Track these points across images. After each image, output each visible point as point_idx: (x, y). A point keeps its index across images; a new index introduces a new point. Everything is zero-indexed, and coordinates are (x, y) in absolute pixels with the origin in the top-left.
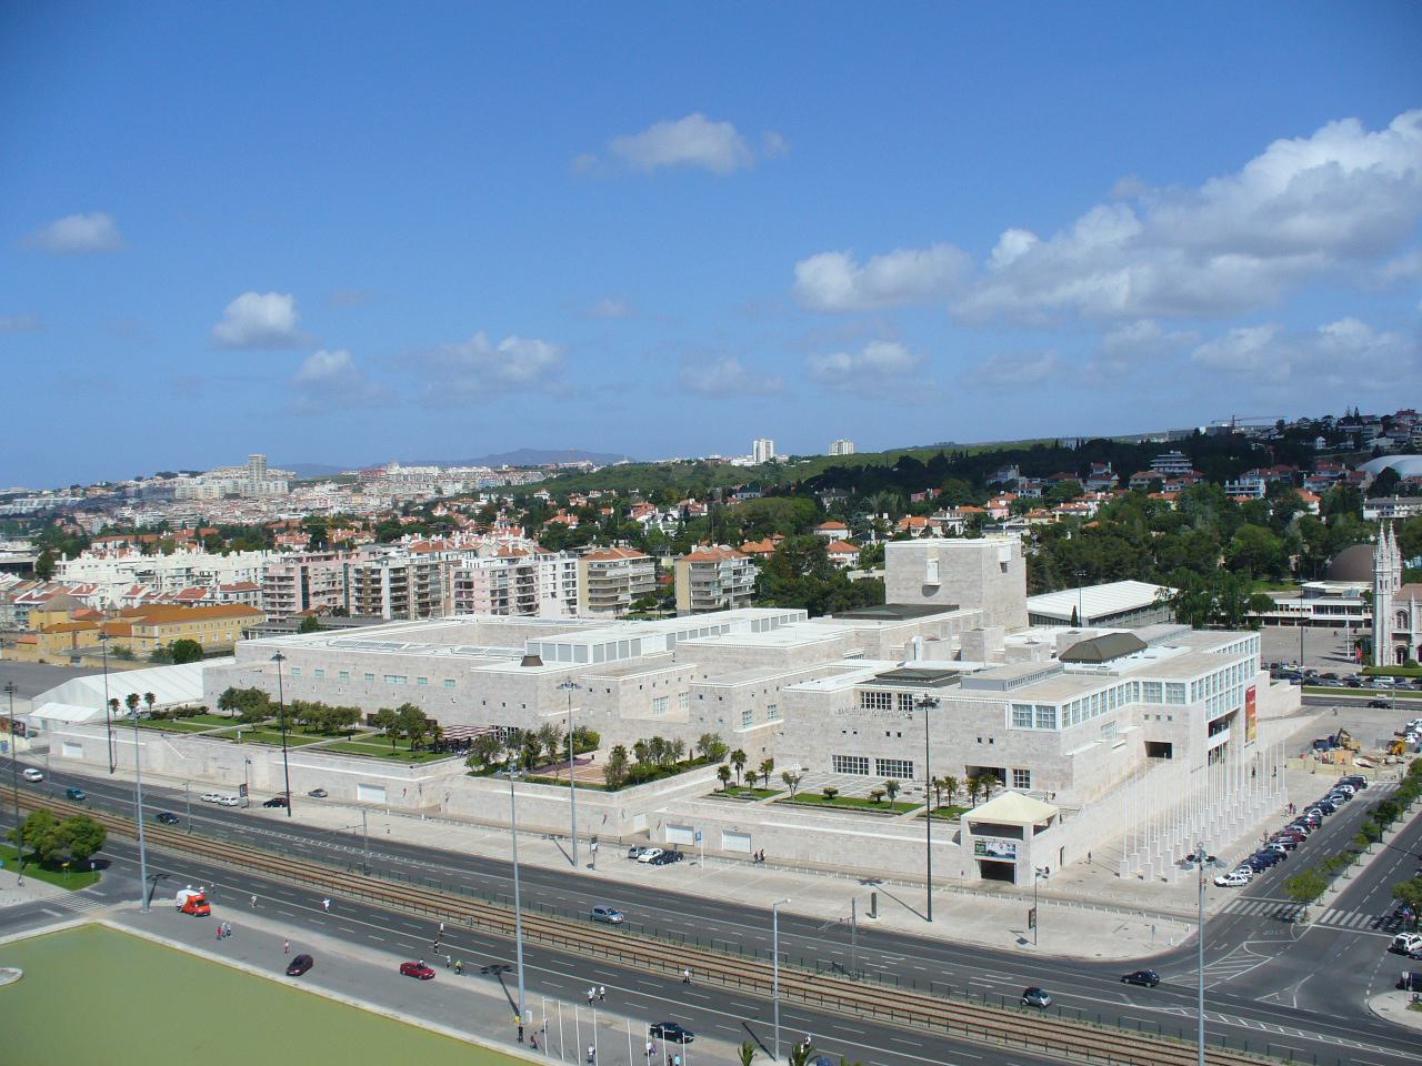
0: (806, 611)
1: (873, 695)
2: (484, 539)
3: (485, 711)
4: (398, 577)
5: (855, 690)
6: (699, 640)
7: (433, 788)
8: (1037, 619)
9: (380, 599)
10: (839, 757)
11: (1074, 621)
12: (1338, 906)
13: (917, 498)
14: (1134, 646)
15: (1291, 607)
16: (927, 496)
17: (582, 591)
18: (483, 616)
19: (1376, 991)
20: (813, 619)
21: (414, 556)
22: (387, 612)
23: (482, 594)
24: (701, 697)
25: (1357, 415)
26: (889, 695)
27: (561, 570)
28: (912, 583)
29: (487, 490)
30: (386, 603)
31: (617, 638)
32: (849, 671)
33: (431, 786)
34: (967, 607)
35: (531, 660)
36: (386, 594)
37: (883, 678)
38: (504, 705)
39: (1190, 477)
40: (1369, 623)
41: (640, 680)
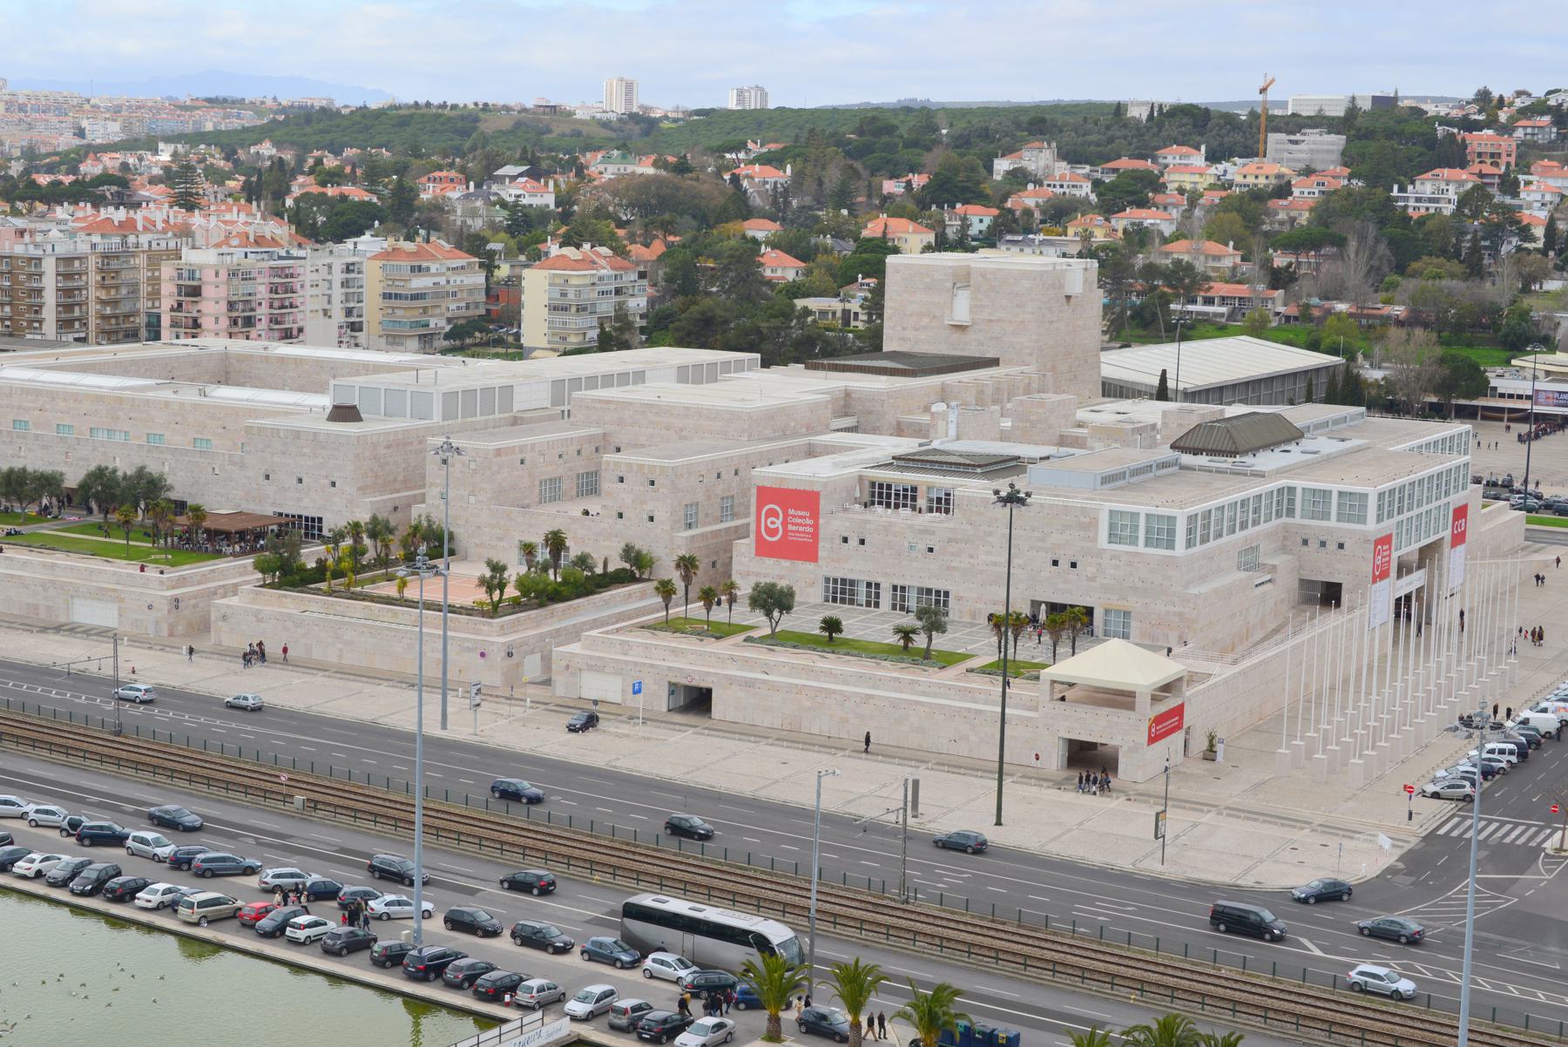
0: (758, 356)
1: (889, 487)
2: (197, 219)
3: (270, 489)
4: (69, 268)
5: (861, 478)
6: (614, 393)
7: (195, 606)
8: (1114, 390)
9: (41, 306)
10: (835, 581)
13: (891, 187)
15: (1500, 391)
16: (909, 183)
17: (372, 309)
18: (214, 342)
20: (774, 368)
21: (96, 239)
22: (50, 328)
23: (212, 307)
24: (621, 480)
26: (914, 489)
27: (338, 276)
28: (925, 321)
29: (168, 140)
30: (50, 314)
31: (478, 383)
32: (852, 449)
33: (193, 602)
34: (1011, 363)
35: (345, 413)
36: (50, 298)
37: (904, 462)
38: (300, 481)
41: (522, 448)
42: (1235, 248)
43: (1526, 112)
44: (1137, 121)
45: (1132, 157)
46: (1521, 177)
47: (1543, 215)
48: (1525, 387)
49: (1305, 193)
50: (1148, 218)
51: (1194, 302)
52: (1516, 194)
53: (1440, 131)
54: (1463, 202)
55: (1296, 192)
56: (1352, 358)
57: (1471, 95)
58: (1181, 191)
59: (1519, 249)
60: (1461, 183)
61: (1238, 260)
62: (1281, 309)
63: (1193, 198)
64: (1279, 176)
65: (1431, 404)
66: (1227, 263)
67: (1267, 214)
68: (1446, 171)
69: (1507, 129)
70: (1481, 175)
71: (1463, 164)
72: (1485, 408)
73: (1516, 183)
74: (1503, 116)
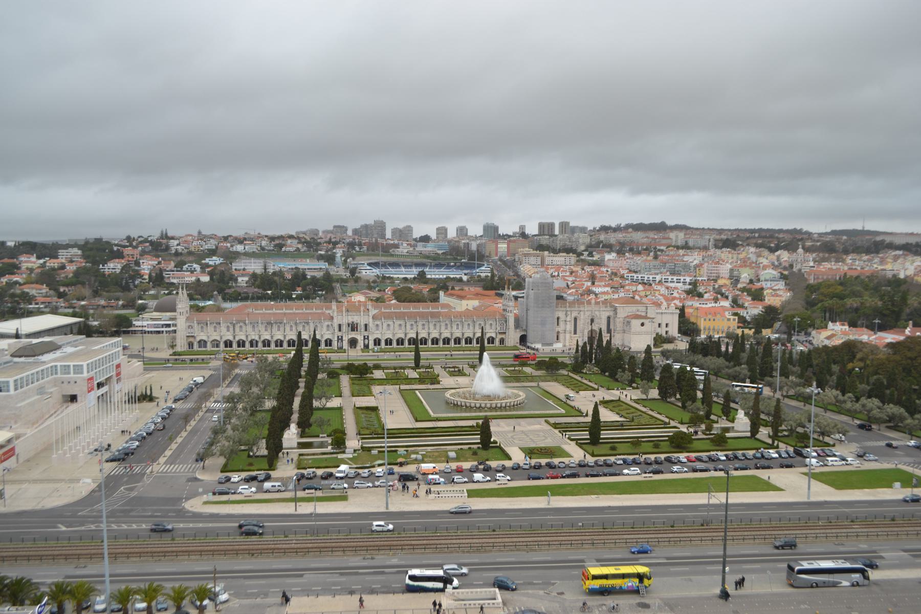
11: (17, 336)
12: (165, 463)
14: (54, 347)
19: (187, 499)
25: (166, 234)
39: (81, 263)
40: (175, 331)
42: (46, 286)
43: (141, 242)
44: (10, 247)
45: (9, 258)
46: (141, 261)
47: (147, 272)
48: (145, 323)
49: (71, 268)
50: (16, 278)
51: (31, 304)
52: (139, 266)
53: (115, 248)
54: (123, 269)
55: (68, 268)
56: (88, 319)
57: (125, 238)
58: (27, 268)
59: (141, 282)
60: (123, 263)
61: (48, 290)
62: (63, 305)
63: (31, 270)
64: (62, 263)
65: (115, 331)
66: (44, 291)
67: (58, 275)
68: (117, 260)
69: (136, 247)
70: (129, 261)
71: (123, 257)
72: (132, 331)
73: (139, 263)
74: (134, 244)
